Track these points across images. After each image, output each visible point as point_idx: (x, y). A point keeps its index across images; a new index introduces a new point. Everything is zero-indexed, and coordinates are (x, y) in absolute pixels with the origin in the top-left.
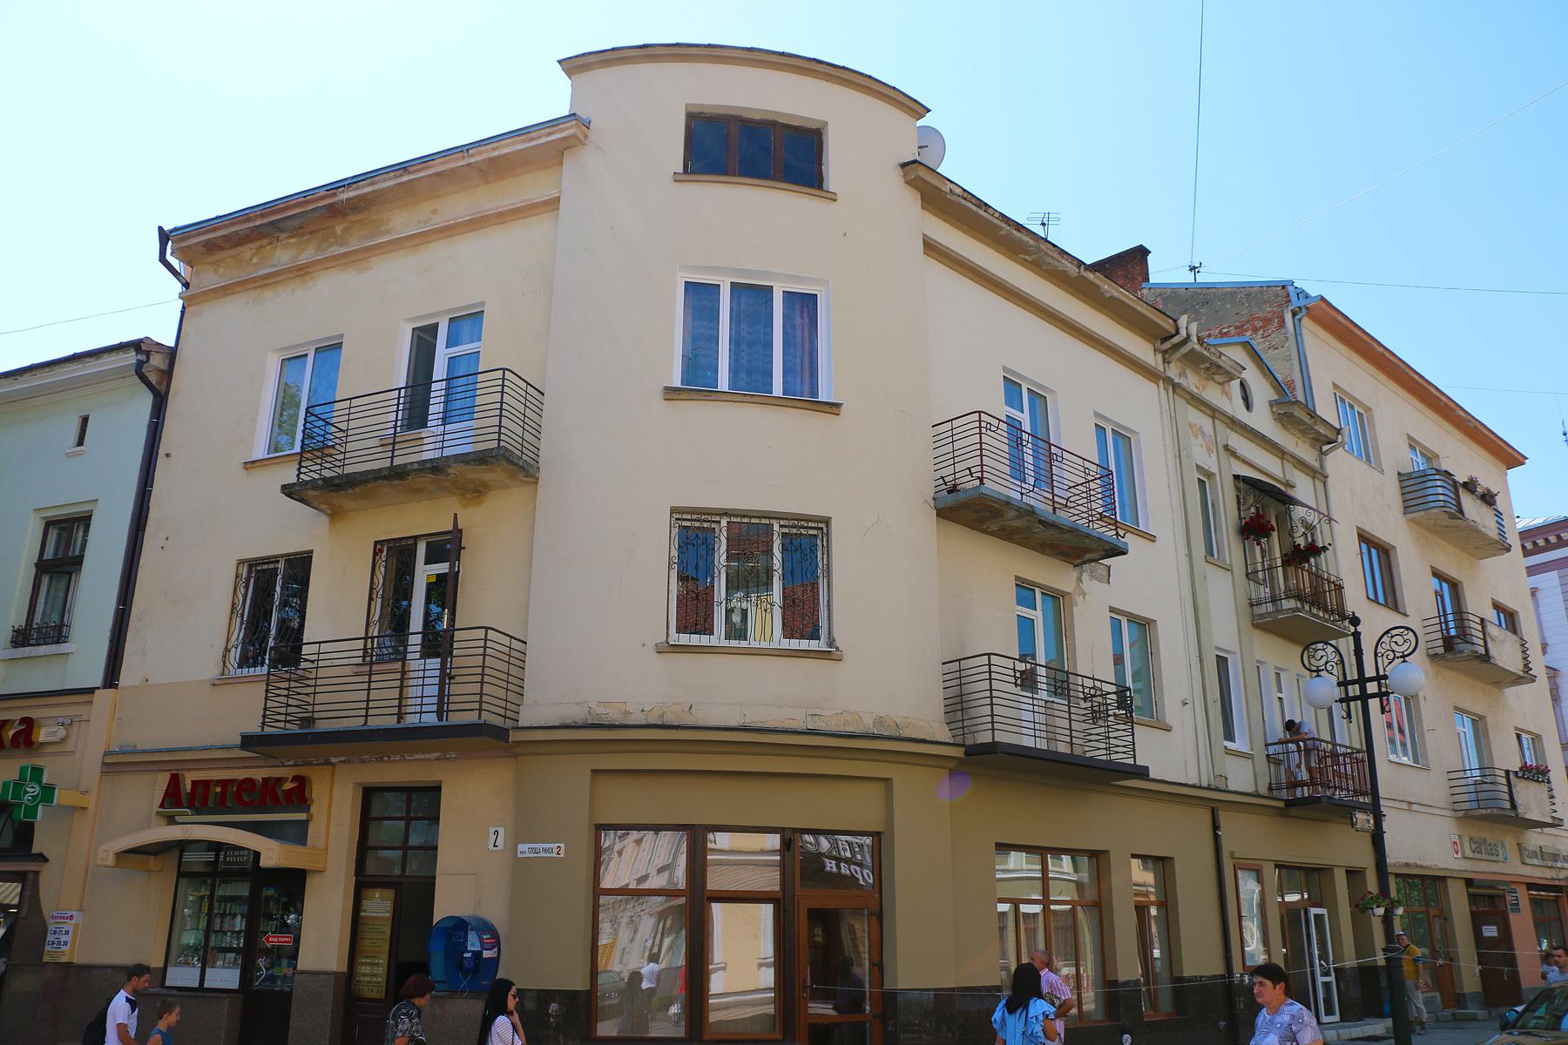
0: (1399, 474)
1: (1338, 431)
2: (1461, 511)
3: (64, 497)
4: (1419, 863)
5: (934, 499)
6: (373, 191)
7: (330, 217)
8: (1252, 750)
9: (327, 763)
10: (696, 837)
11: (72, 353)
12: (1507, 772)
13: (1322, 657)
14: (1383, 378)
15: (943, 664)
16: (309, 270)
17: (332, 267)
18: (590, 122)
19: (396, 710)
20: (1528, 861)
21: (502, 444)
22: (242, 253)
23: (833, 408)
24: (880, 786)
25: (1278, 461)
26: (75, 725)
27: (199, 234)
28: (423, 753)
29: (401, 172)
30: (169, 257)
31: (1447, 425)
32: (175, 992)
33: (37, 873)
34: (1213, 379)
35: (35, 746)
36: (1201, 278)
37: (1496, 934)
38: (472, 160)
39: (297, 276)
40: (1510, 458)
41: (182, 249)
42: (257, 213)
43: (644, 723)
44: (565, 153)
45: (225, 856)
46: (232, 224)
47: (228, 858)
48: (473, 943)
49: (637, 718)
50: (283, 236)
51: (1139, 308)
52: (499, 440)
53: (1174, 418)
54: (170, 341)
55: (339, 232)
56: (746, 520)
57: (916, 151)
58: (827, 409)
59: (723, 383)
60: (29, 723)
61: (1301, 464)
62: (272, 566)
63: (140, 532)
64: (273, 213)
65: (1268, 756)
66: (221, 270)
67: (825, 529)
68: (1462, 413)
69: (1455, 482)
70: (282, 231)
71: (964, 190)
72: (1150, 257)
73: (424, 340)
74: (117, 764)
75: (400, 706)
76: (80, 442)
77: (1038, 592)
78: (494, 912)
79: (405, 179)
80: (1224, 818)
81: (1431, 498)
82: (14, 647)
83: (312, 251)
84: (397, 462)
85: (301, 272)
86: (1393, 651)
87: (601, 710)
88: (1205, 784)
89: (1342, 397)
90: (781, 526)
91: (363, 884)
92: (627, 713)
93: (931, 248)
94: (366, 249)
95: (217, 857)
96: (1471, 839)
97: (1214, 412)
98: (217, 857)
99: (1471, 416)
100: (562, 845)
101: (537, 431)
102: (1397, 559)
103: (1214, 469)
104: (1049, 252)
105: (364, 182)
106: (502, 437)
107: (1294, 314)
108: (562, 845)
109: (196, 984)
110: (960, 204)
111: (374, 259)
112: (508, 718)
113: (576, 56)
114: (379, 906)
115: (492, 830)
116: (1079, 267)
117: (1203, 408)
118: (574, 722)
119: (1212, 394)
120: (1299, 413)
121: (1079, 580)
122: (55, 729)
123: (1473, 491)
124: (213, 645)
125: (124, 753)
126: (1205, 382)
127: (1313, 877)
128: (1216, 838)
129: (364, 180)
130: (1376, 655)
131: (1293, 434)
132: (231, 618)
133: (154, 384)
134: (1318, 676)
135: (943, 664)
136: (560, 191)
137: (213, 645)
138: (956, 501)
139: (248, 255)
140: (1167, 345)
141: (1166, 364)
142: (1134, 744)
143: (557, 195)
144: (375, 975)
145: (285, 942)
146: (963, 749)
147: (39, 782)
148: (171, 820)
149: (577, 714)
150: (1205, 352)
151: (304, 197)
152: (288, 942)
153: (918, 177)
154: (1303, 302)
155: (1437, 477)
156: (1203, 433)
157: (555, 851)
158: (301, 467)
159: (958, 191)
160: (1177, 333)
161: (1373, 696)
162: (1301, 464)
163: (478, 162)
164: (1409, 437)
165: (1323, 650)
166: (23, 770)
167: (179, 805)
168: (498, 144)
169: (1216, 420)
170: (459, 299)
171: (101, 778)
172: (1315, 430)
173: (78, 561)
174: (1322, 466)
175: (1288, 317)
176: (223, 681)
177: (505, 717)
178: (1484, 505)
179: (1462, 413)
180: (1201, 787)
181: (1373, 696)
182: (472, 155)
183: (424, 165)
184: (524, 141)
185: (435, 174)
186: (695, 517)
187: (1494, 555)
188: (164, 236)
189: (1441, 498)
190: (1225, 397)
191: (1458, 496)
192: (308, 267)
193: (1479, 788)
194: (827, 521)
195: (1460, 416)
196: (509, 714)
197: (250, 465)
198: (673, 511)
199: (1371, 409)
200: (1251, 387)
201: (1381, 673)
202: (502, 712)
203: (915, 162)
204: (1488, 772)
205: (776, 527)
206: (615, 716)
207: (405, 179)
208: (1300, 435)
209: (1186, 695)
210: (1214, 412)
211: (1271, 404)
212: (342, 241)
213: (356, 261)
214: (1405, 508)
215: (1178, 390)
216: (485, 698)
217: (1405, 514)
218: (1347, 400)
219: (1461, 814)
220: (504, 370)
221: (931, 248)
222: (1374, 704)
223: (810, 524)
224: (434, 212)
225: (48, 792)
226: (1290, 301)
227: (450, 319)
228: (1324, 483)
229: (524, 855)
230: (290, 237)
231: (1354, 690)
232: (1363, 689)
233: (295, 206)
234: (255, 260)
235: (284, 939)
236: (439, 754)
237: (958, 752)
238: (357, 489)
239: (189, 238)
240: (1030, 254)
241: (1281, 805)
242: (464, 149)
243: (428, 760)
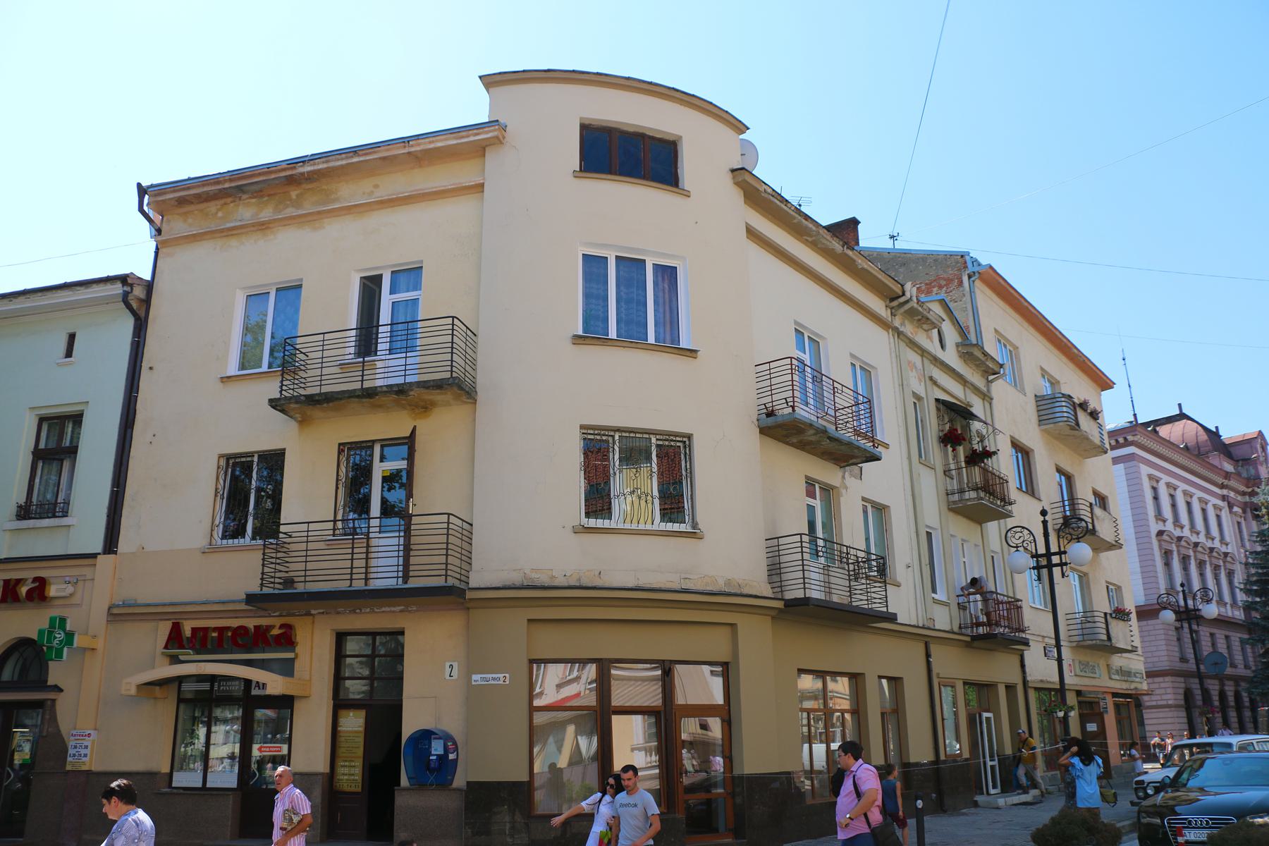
0: (1036, 396)
1: (1001, 366)
2: (1078, 424)
3: (59, 399)
4: (1049, 679)
5: (758, 420)
6: (328, 168)
7: (287, 184)
8: (949, 599)
9: (308, 614)
10: (604, 666)
11: (63, 282)
12: (1105, 614)
13: (1020, 537)
14: (1026, 324)
15: (766, 540)
16: (271, 225)
17: (289, 225)
18: (506, 126)
19: (363, 576)
20: (1113, 677)
21: (454, 375)
22: (208, 207)
23: (692, 353)
24: (727, 630)
25: (961, 387)
26: (80, 583)
27: (175, 191)
28: (389, 606)
29: (351, 154)
30: (146, 208)
31: (1065, 359)
32: (181, 791)
33: (54, 701)
34: (922, 327)
35: (48, 600)
36: (901, 245)
37: (1096, 729)
38: (412, 149)
39: (258, 230)
40: (1104, 383)
41: (157, 202)
43: (566, 585)
44: (487, 149)
45: (219, 687)
46: (204, 185)
47: (221, 688)
48: (437, 748)
49: (561, 581)
50: (245, 196)
51: (880, 277)
52: (452, 371)
53: (898, 357)
54: (147, 276)
55: (294, 197)
56: (632, 435)
57: (739, 158)
58: (688, 353)
59: (613, 334)
60: (42, 583)
61: (976, 390)
62: (249, 459)
63: (129, 430)
64: (240, 179)
65: (959, 604)
66: (190, 220)
67: (687, 443)
68: (1075, 351)
69: (1074, 403)
70: (244, 192)
71: (774, 190)
72: (860, 227)
73: (371, 287)
74: (120, 614)
75: (366, 573)
76: (69, 354)
77: (817, 486)
78: (452, 724)
79: (355, 160)
80: (933, 648)
81: (1058, 415)
82: (18, 520)
83: (271, 210)
84: (367, 385)
85: (263, 227)
86: (1071, 534)
87: (534, 575)
88: (921, 625)
89: (1001, 339)
90: (657, 440)
91: (340, 704)
92: (553, 577)
93: (752, 233)
94: (319, 213)
95: (212, 686)
96: (1080, 662)
97: (923, 352)
98: (212, 686)
99: (1081, 353)
101: (474, 363)
102: (1035, 458)
103: (923, 395)
104: (825, 236)
105: (319, 160)
106: (454, 369)
107: (970, 277)
108: (507, 675)
109: (200, 785)
110: (770, 200)
111: (326, 220)
112: (463, 581)
113: (494, 74)
114: (354, 722)
115: (448, 664)
116: (843, 247)
117: (916, 349)
118: (513, 584)
119: (921, 339)
120: (978, 353)
121: (843, 477)
122: (64, 586)
123: (1085, 410)
124: (201, 522)
125: (130, 606)
126: (916, 330)
127: (983, 689)
128: (929, 663)
129: (320, 158)
130: (1023, 528)
131: (971, 367)
132: (215, 501)
133: (135, 308)
134: (1017, 550)
135: (766, 540)
136: (484, 179)
137: (201, 522)
138: (776, 422)
139: (213, 209)
140: (895, 303)
141: (893, 317)
142: (886, 597)
143: (481, 181)
144: (353, 775)
146: (783, 603)
147: (64, 630)
148: (175, 660)
149: (516, 578)
150: (920, 309)
151: (268, 168)
153: (745, 181)
154: (976, 269)
155: (1063, 399)
156: (916, 368)
157: (502, 679)
158: (282, 385)
159: (769, 190)
160: (904, 294)
161: (1056, 565)
162: (976, 390)
163: (417, 151)
164: (1042, 369)
165: (1021, 532)
166: (52, 620)
167: (182, 647)
168: (434, 139)
169: (924, 358)
170: (404, 256)
171: (107, 627)
172: (985, 364)
173: (73, 451)
174: (988, 391)
175: (965, 279)
176: (211, 549)
177: (460, 580)
178: (1092, 419)
179: (1075, 351)
180: (918, 627)
181: (1056, 565)
182: (412, 146)
183: (373, 150)
185: (380, 158)
186: (596, 432)
187: (1096, 456)
188: (142, 191)
189: (1065, 414)
190: (928, 340)
191: (1076, 413)
192: (269, 223)
193: (1084, 626)
194: (690, 437)
195: (1074, 353)
196: (463, 578)
197: (226, 379)
198: (582, 427)
199: (1017, 348)
200: (945, 333)
201: (1062, 549)
202: (458, 576)
203: (742, 169)
204: (1089, 614)
205: (654, 440)
206: (545, 580)
207: (355, 160)
208: (974, 368)
209: (908, 561)
210: (923, 352)
211: (957, 345)
212: (297, 204)
213: (311, 221)
214: (1040, 421)
215: (901, 336)
216: (449, 567)
217: (1039, 425)
218: (1002, 341)
219: (1074, 644)
220: (453, 317)
221: (752, 233)
222: (1057, 571)
223: (678, 439)
224: (376, 186)
225: (70, 636)
226: (967, 267)
227: (392, 272)
228: (990, 404)
229: (478, 683)
230: (251, 198)
231: (1044, 562)
232: (1049, 560)
233: (260, 174)
234: (220, 214)
236: (402, 607)
237: (780, 604)
238: (331, 404)
239: (165, 193)
240: (811, 236)
241: (968, 639)
242: (406, 140)
243: (394, 612)
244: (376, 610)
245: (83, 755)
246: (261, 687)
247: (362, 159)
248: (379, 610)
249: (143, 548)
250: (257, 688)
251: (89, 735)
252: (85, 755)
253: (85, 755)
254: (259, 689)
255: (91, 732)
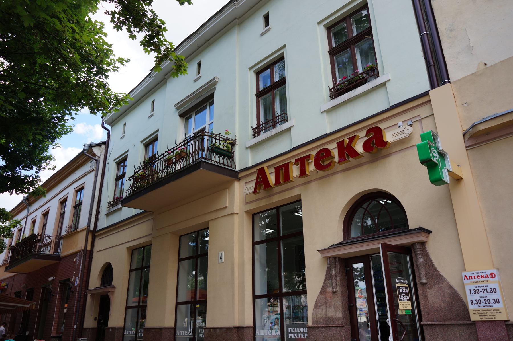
33: (423, 244)
245: (492, 301)
251: (492, 275)
252: (497, 301)
253: (497, 301)
255: (495, 271)
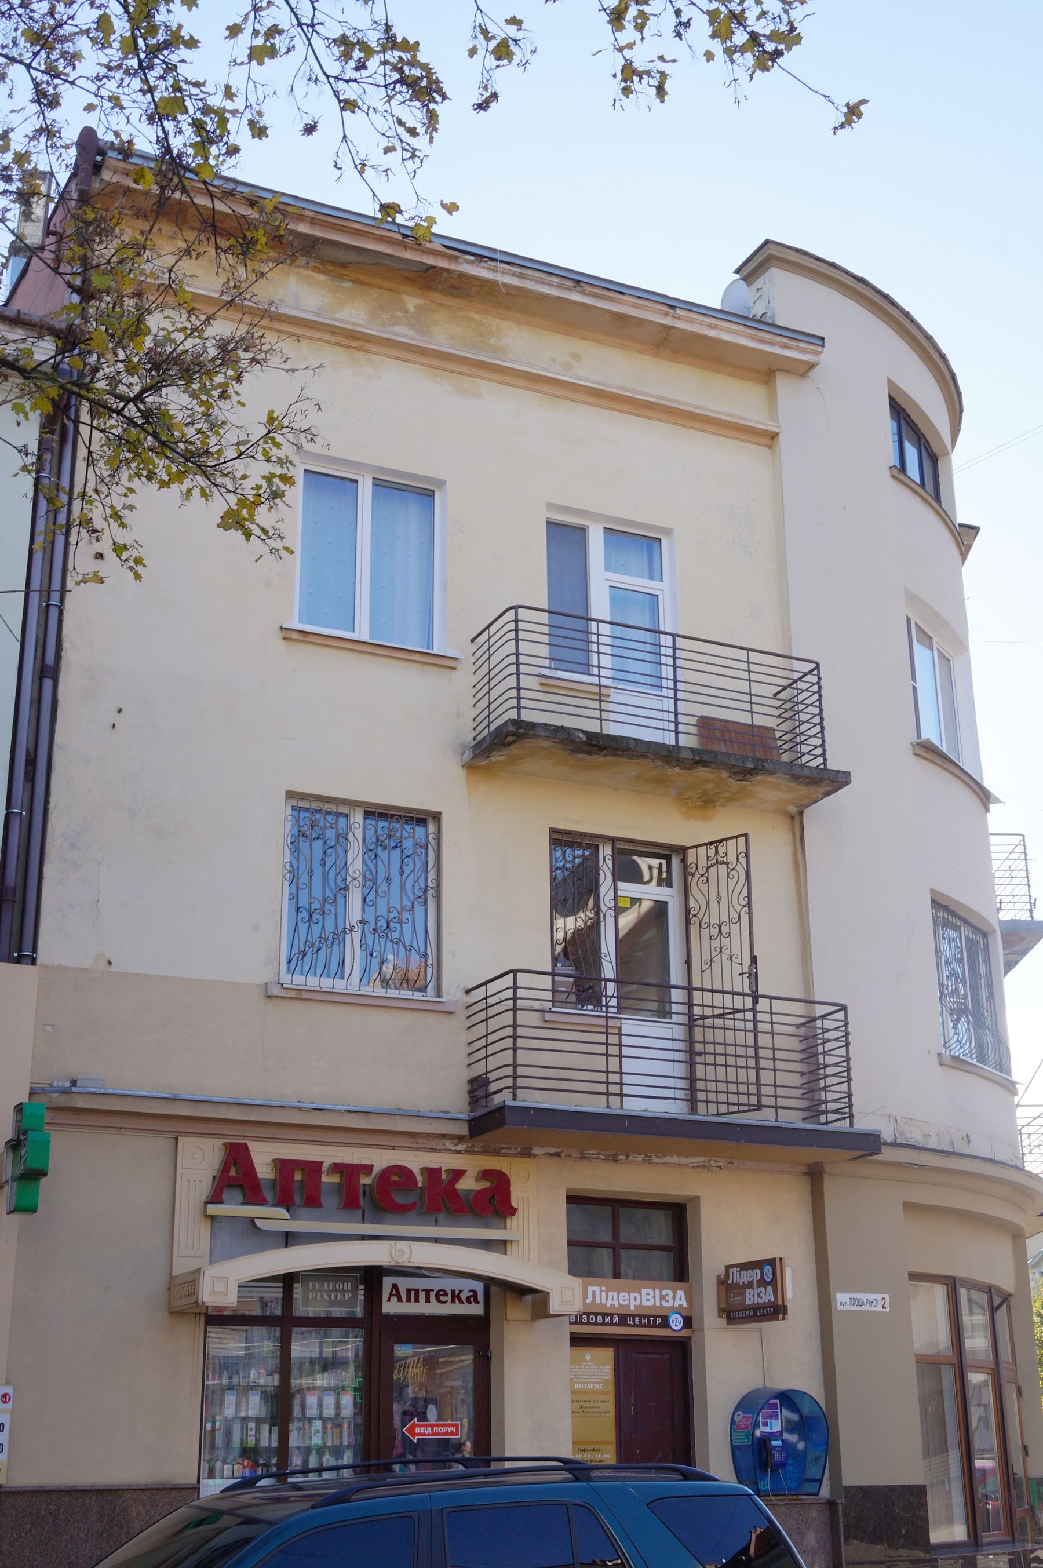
16: (368, 346)
17: (408, 361)
28: (679, 1155)
39: (336, 344)
42: (307, 213)
63: (48, 683)
64: (334, 227)
92: (927, 1135)
100: (887, 1297)
108: (887, 1297)
113: (790, 248)
124: (256, 927)
129: (508, 263)
137: (256, 927)
145: (446, 1433)
152: (452, 1433)
157: (881, 1303)
182: (679, 318)
184: (753, 338)
224: (576, 357)
229: (845, 1308)
235: (445, 1429)
244: (655, 1159)
246: (404, 1297)
247: (587, 300)
248: (659, 1160)
249: (110, 963)
250: (394, 1299)
254: (400, 1300)
